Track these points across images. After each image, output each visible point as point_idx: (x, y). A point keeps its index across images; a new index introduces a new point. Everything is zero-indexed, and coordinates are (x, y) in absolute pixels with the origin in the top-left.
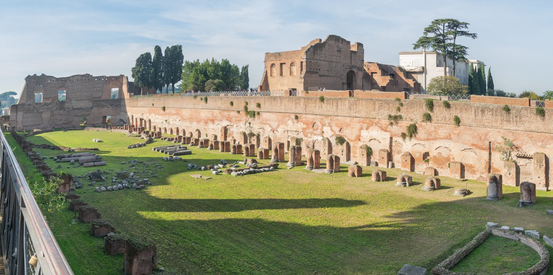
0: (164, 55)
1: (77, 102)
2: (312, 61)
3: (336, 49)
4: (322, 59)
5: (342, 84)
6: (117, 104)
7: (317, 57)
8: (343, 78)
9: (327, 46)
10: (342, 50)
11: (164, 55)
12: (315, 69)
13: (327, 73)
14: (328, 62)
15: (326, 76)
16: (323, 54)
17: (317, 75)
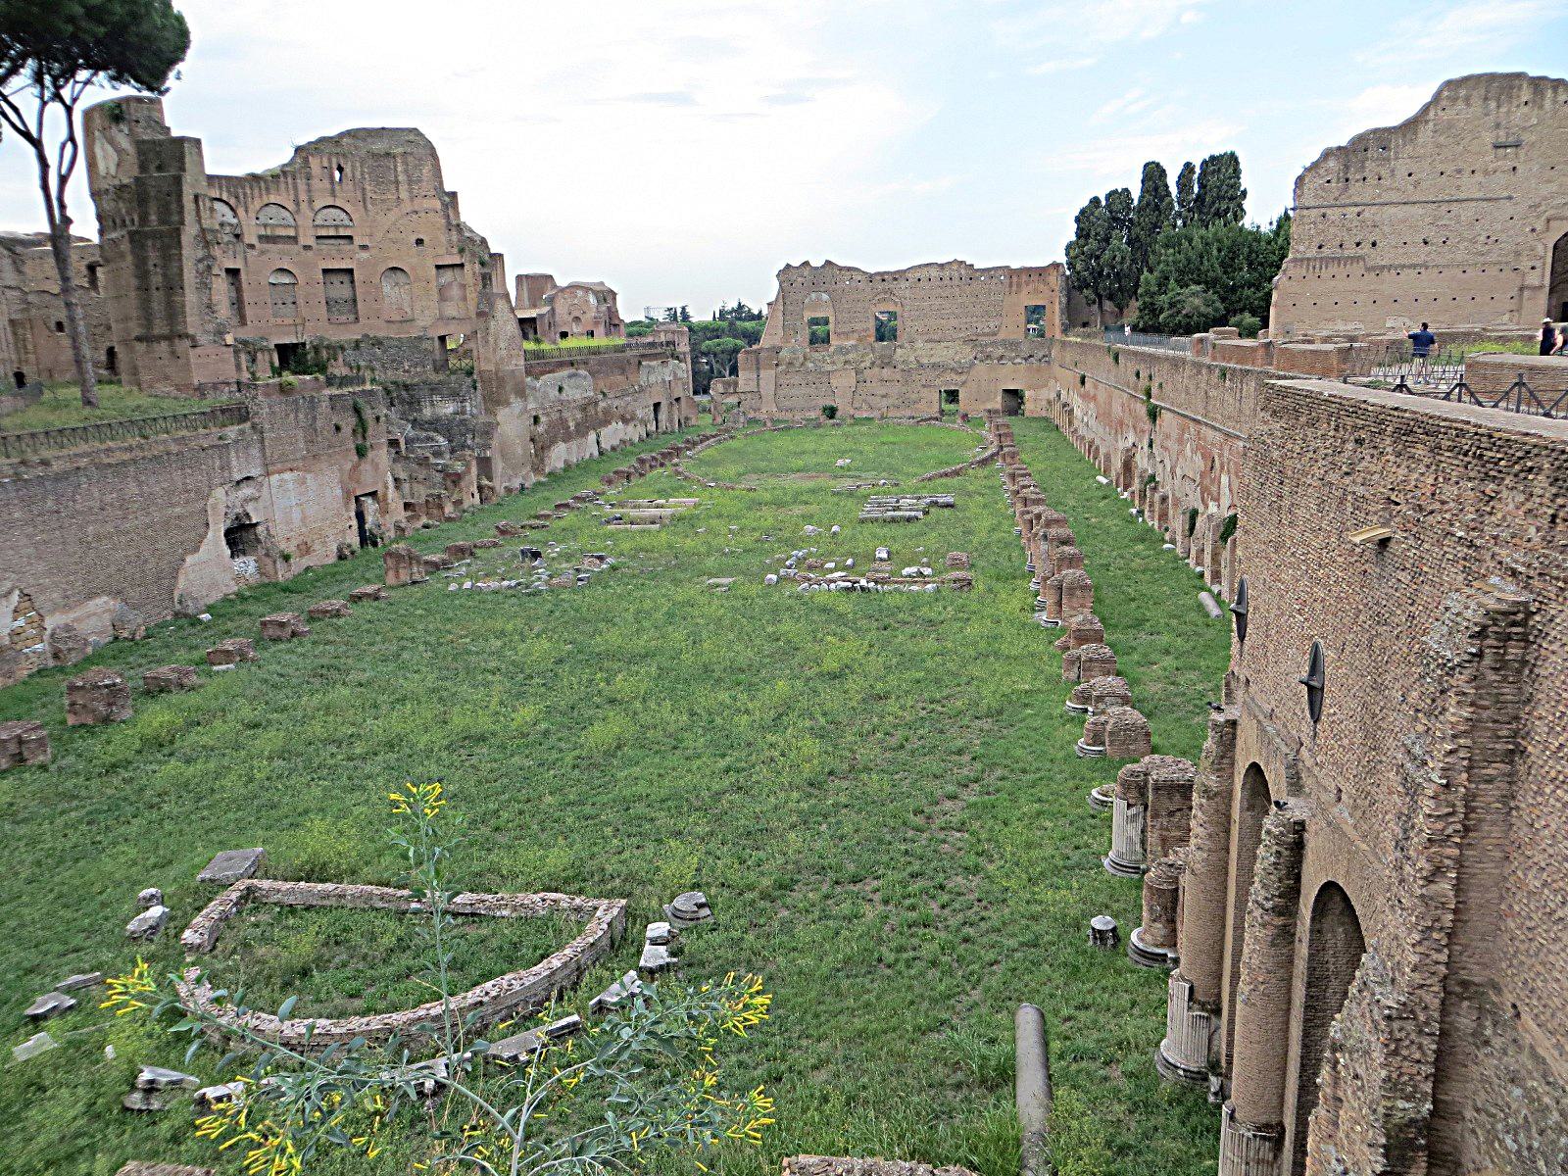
0: (1174, 190)
1: (929, 345)
2: (1334, 214)
3: (1488, 138)
4: (1385, 198)
5: (1514, 292)
6: (1041, 354)
7: (1358, 192)
8: (1525, 264)
9: (1425, 134)
10: (1528, 138)
11: (1174, 190)
12: (1349, 244)
13: (1422, 254)
14: (1434, 206)
15: (1414, 266)
16: (1402, 172)
17: (1357, 269)
